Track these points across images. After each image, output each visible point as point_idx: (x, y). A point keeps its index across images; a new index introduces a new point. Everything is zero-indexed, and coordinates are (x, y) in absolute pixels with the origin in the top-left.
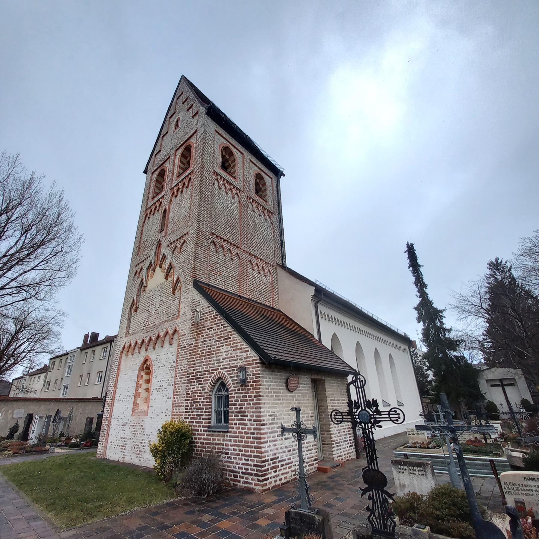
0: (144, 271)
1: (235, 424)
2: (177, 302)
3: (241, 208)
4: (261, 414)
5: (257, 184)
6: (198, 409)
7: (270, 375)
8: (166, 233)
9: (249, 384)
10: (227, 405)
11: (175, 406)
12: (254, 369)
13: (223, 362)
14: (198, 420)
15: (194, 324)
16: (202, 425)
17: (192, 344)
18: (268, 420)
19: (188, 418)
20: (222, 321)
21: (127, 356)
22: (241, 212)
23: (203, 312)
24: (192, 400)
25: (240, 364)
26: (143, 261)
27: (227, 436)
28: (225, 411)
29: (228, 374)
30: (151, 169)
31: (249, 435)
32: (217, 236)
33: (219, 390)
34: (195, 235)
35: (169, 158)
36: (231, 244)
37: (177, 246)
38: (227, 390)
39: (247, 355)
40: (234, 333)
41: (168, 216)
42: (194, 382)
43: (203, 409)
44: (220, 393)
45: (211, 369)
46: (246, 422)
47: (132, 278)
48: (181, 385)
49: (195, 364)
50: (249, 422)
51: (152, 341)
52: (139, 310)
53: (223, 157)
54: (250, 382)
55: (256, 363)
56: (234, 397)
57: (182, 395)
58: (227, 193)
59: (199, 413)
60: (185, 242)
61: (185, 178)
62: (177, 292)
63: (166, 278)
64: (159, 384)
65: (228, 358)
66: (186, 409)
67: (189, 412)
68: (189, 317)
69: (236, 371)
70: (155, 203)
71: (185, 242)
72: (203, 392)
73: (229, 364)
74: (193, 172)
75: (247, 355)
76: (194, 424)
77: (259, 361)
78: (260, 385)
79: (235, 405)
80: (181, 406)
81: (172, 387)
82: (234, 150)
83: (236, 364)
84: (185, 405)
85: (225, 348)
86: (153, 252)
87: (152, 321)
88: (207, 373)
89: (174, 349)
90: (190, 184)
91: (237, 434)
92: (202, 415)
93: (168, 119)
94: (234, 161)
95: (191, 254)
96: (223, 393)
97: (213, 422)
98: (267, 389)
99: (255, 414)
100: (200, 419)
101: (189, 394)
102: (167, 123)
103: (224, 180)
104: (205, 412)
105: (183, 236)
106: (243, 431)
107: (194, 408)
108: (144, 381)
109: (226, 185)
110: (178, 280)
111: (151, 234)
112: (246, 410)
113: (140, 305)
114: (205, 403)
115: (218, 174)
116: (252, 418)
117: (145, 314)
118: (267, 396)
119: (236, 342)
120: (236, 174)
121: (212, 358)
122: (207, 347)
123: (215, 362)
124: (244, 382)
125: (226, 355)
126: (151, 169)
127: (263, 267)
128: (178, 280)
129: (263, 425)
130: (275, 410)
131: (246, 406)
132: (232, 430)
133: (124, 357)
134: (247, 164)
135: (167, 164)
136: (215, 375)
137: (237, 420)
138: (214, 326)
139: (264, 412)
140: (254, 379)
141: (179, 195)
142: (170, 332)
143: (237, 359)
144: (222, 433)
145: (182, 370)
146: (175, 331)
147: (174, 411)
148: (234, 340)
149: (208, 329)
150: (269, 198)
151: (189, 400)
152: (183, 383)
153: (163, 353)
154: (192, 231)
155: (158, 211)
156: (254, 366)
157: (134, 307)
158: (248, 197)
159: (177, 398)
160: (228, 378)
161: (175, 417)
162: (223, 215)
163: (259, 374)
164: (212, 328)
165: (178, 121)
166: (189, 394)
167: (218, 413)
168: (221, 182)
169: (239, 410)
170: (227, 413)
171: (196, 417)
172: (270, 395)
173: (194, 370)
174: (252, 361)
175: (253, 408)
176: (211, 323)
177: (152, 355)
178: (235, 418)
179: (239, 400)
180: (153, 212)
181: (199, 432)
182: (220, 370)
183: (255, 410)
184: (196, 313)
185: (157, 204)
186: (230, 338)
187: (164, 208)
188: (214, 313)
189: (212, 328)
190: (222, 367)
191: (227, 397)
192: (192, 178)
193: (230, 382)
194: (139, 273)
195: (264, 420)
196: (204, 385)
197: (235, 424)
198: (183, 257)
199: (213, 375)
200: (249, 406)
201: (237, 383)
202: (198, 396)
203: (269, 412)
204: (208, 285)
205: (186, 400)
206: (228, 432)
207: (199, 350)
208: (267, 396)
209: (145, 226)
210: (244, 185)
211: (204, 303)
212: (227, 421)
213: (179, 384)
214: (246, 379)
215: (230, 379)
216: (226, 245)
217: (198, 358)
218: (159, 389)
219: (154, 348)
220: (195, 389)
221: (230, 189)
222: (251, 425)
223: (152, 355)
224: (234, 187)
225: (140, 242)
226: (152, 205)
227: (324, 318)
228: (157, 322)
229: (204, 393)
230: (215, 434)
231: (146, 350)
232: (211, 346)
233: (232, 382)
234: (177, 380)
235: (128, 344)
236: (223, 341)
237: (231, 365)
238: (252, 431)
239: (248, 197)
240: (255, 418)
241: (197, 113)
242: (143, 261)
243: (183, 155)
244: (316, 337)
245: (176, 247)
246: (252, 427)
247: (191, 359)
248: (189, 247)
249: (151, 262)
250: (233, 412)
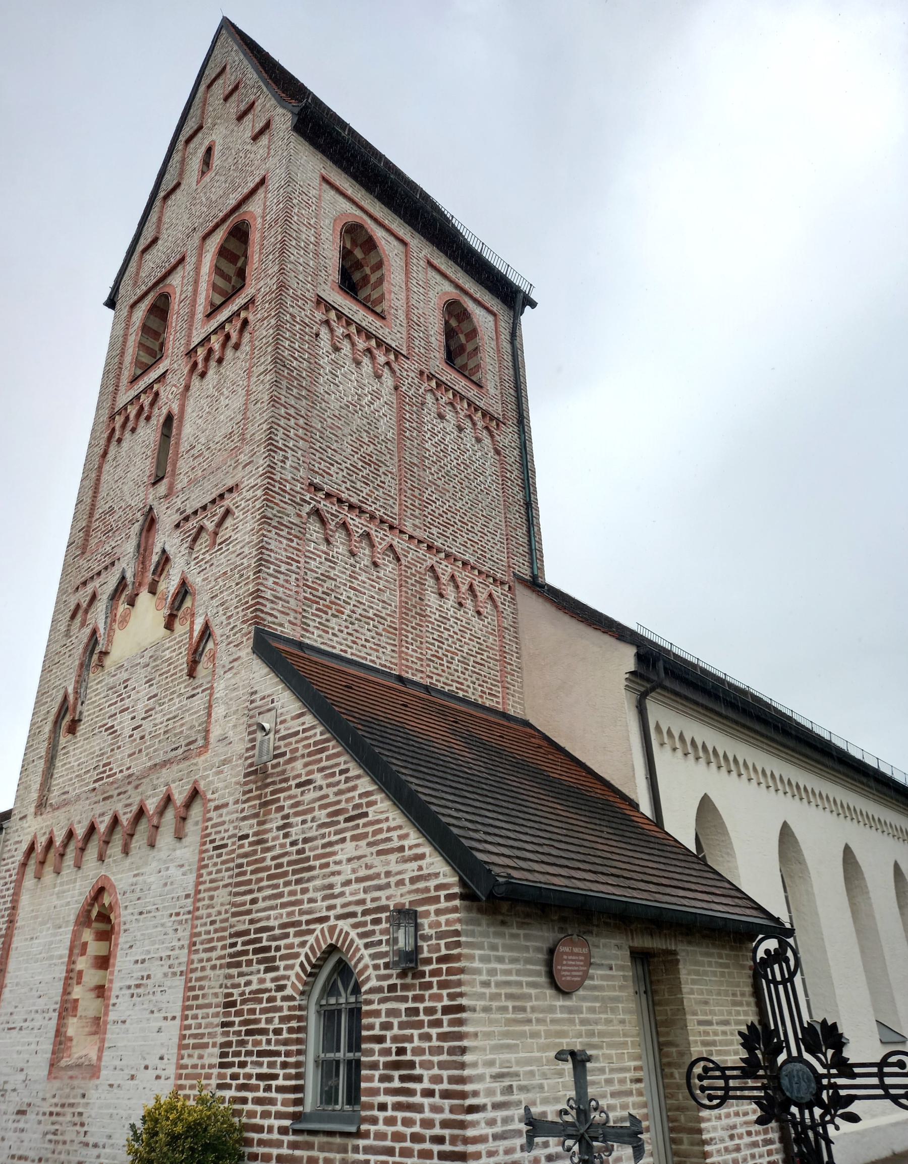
0: (101, 606)
1: (383, 1107)
2: (199, 702)
3: (400, 409)
4: (466, 1072)
5: (450, 333)
6: (261, 1054)
7: (497, 934)
8: (171, 487)
9: (427, 969)
10: (355, 1043)
11: (186, 1047)
12: (442, 918)
13: (342, 894)
14: (261, 1094)
15: (255, 772)
16: (273, 1109)
17: (246, 837)
18: (490, 1092)
19: (228, 1087)
20: (342, 759)
21: (38, 877)
22: (401, 419)
23: (283, 733)
24: (242, 1023)
25: (398, 900)
26: (99, 574)
27: (356, 1149)
28: (349, 1062)
29: (362, 936)
30: (128, 294)
31: (427, 1146)
32: (328, 496)
33: (330, 990)
34: (259, 493)
35: (182, 260)
36: (372, 517)
37: (204, 526)
38: (356, 990)
39: (420, 868)
40: (378, 797)
41: (179, 434)
42: (249, 963)
43: (277, 1054)
44: (333, 1001)
45: (304, 918)
46: (418, 1099)
47: (63, 628)
48: (209, 972)
49: (254, 901)
50: (426, 1101)
51: (119, 828)
52: (82, 728)
53: (346, 254)
54: (428, 961)
55: (449, 897)
56: (377, 1014)
57: (209, 1006)
58: (358, 363)
59: (265, 1070)
60: (228, 512)
61: (229, 320)
62: (202, 670)
63: (169, 625)
64: (139, 971)
65: (359, 880)
66: (223, 1055)
67: (232, 1065)
68: (239, 747)
69: (384, 925)
70: (138, 397)
71: (228, 512)
72: (279, 995)
73: (362, 902)
74: (252, 301)
75: (420, 868)
76: (250, 1106)
77: (456, 890)
78: (462, 971)
79: (380, 1039)
80: (205, 1046)
81: (180, 982)
82: (379, 234)
83: (384, 902)
84: (221, 1039)
85: (349, 849)
86: (130, 547)
87: (121, 762)
88: (291, 931)
89: (188, 851)
90: (246, 337)
91: (388, 1143)
92: (275, 1077)
93: (180, 145)
94: (379, 265)
95: (246, 550)
96: (342, 1000)
97: (311, 1100)
98: (486, 984)
99: (445, 1074)
100: (268, 1088)
101: (233, 1004)
102: (176, 157)
103: (349, 322)
104: (284, 1065)
105: (222, 496)
106: (408, 1131)
107: (249, 1053)
108: (91, 961)
109: (356, 338)
110: (206, 633)
111: (125, 488)
112: (417, 1059)
113: (89, 713)
114: (285, 1035)
115: (329, 307)
116: (437, 1087)
117: (102, 741)
118: (486, 1009)
119: (384, 826)
120: (385, 305)
121: (309, 880)
122: (293, 844)
123: (319, 895)
124: (409, 963)
125: (354, 871)
126: (128, 294)
127: (471, 588)
128: (206, 633)
129: (472, 1109)
130: (512, 1056)
131: (416, 1043)
132: (373, 1128)
133: (29, 882)
134: (419, 272)
135: (176, 280)
136: (318, 938)
137: (388, 1092)
138: (317, 776)
139: (474, 1065)
140: (444, 952)
141: (211, 373)
142: (179, 798)
143: (388, 886)
144: (338, 1140)
145: (213, 923)
146: (195, 793)
147: (186, 1061)
148: (378, 822)
149: (298, 786)
150: (489, 376)
151: (232, 1024)
152: (214, 967)
153: (154, 865)
154: (251, 479)
155: (148, 418)
156: (443, 904)
157: (68, 718)
158: (422, 373)
159: (195, 1017)
160: (357, 949)
161: (188, 1083)
162: (347, 431)
163: (457, 933)
164: (309, 782)
166: (233, 1004)
167: (328, 1069)
168: (340, 331)
169: (394, 1058)
170: (355, 1067)
171: (253, 1081)
172: (495, 1004)
173: (252, 922)
174: (438, 888)
175: (439, 1051)
176: (306, 765)
177: (121, 874)
178: (383, 1086)
179: (396, 1021)
180: (130, 424)
181: (265, 1136)
182: (332, 922)
183: (445, 1057)
184: (259, 735)
185: (146, 400)
186: (365, 815)
187: (165, 411)
188: (318, 733)
189: (309, 782)
190: (339, 911)
191: (355, 1014)
192: (251, 318)
193: (367, 960)
194: (86, 611)
195: (475, 1094)
196: (281, 972)
197: (383, 1107)
198: (222, 561)
199: (311, 939)
200: (426, 1045)
201: (387, 966)
202: (264, 1011)
203: (491, 1063)
204: (301, 645)
205: (224, 1025)
206: (359, 1135)
207: (269, 855)
208: (486, 1009)
209: (106, 467)
210: (410, 338)
211: (287, 703)
212: (354, 1094)
213: (203, 969)
214: (417, 949)
215: (366, 953)
216: (356, 523)
217: (265, 883)
218: (138, 986)
219: (126, 851)
220: (254, 986)
221: (369, 350)
222: (435, 1109)
223: (121, 874)
224: (380, 343)
225: (91, 515)
226: (131, 402)
227: (668, 747)
228: (139, 765)
229: (284, 999)
230: (317, 1140)
231: (101, 858)
232: (306, 841)
233: (371, 963)
234: (195, 957)
235: (42, 841)
236: (343, 825)
237: (369, 905)
238: (437, 1131)
239: (422, 373)
240: (445, 1086)
241: (267, 126)
242: (99, 574)
243: (223, 252)
244: (646, 808)
245: (202, 529)
246: (438, 1117)
247: (241, 886)
248: (243, 529)
249: (123, 578)
250: (374, 1066)
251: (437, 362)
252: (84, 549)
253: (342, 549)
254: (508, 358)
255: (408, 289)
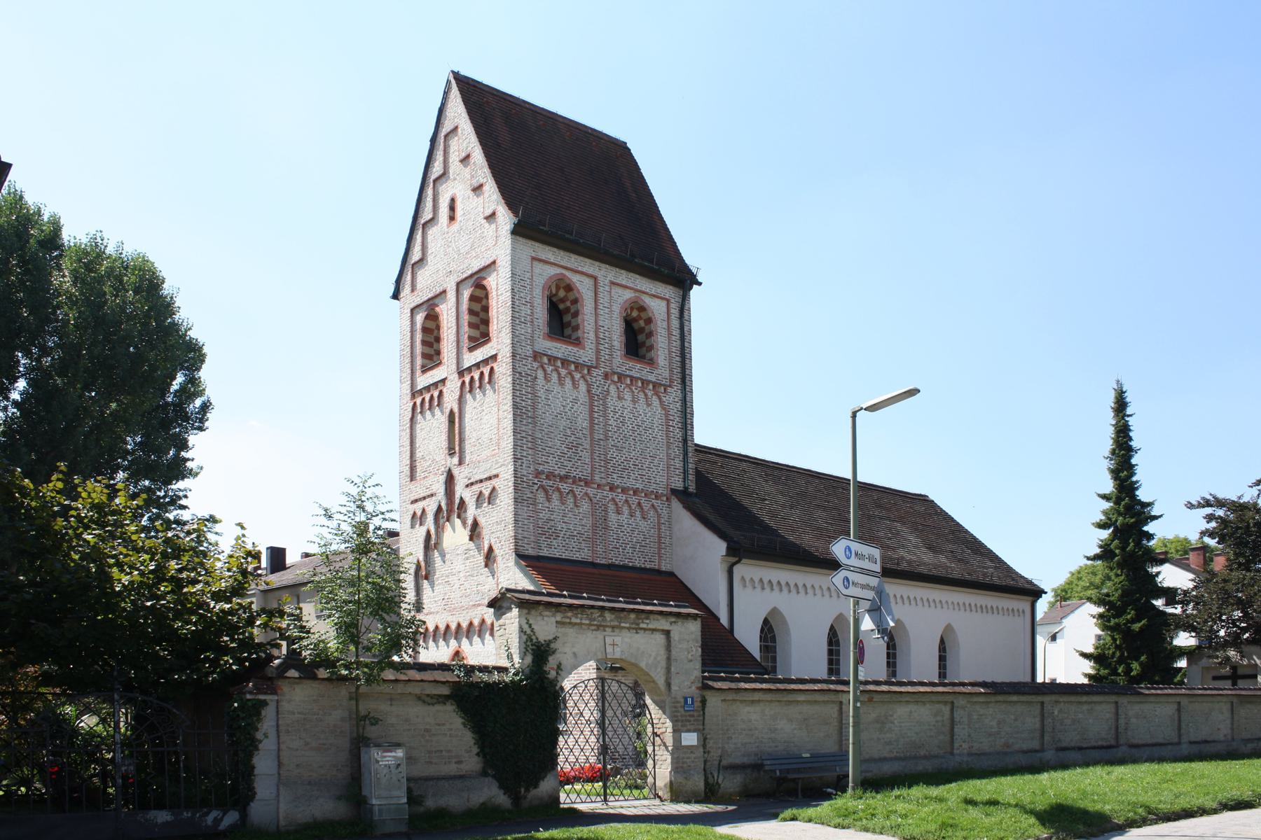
3: (591, 406)
94: (575, 301)
120: (580, 333)
165: (453, 200)
216: (565, 487)
243: (473, 298)
251: (619, 360)
252: (412, 477)
253: (557, 503)
254: (676, 332)
255: (596, 315)
